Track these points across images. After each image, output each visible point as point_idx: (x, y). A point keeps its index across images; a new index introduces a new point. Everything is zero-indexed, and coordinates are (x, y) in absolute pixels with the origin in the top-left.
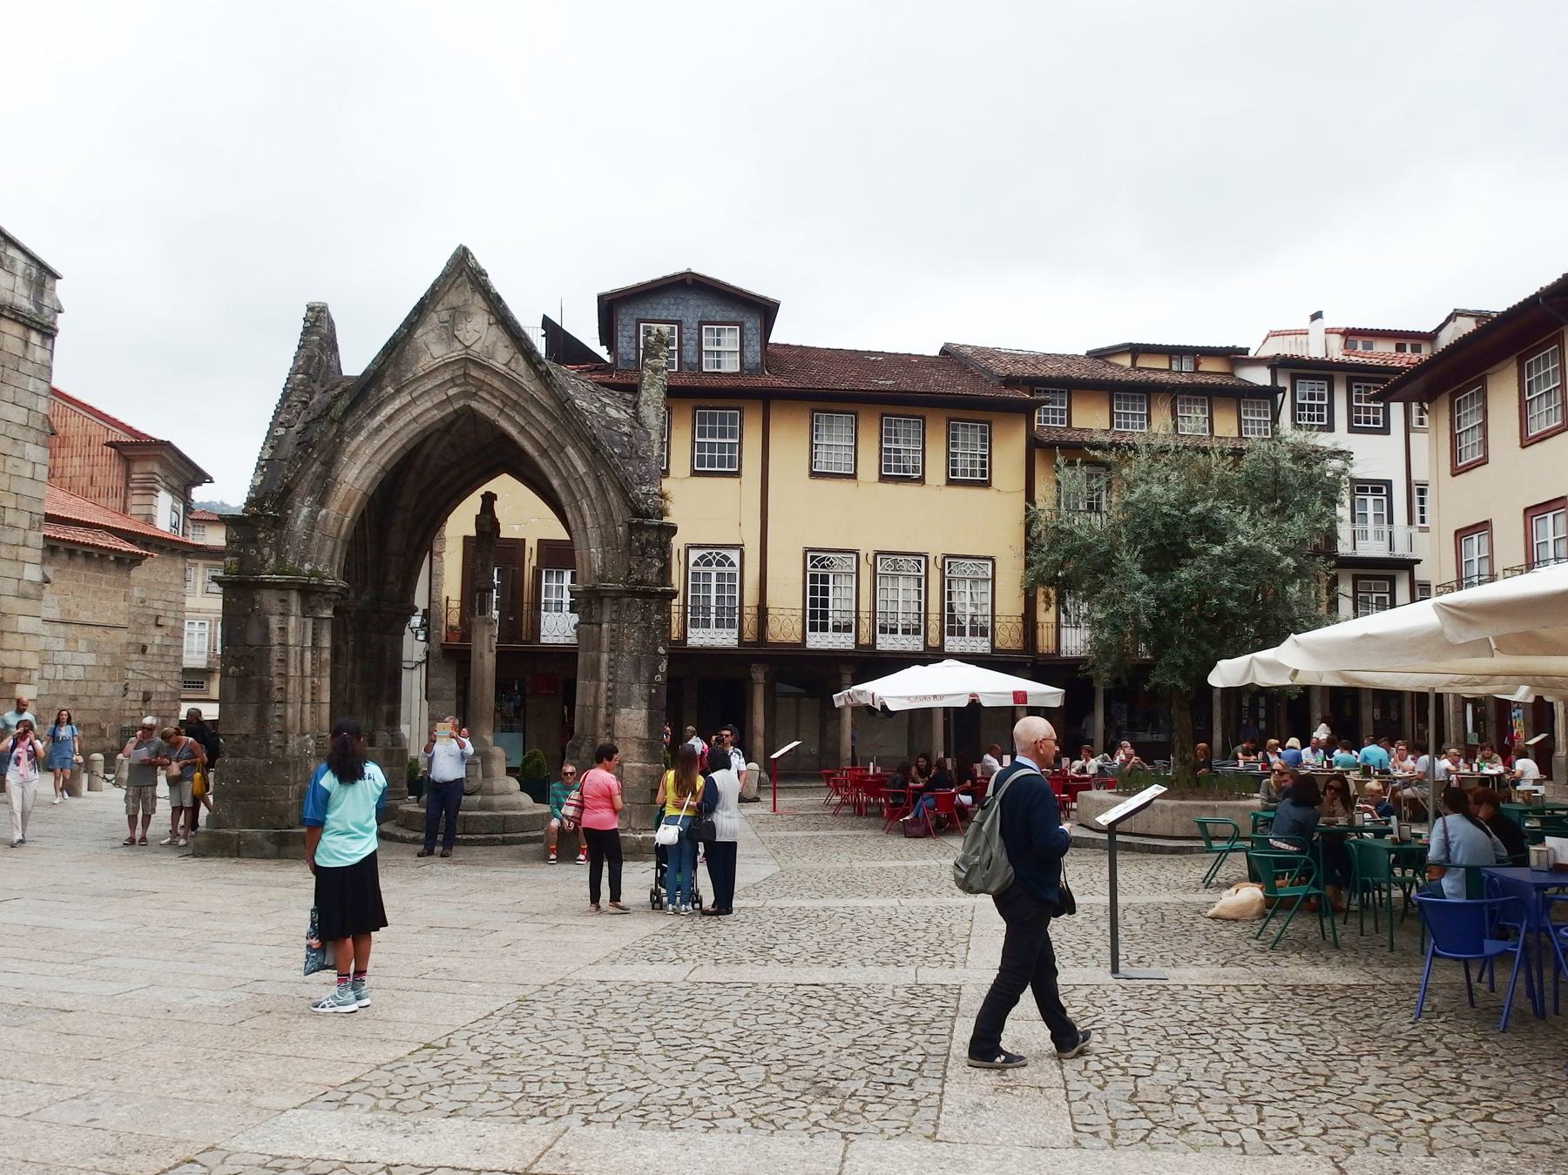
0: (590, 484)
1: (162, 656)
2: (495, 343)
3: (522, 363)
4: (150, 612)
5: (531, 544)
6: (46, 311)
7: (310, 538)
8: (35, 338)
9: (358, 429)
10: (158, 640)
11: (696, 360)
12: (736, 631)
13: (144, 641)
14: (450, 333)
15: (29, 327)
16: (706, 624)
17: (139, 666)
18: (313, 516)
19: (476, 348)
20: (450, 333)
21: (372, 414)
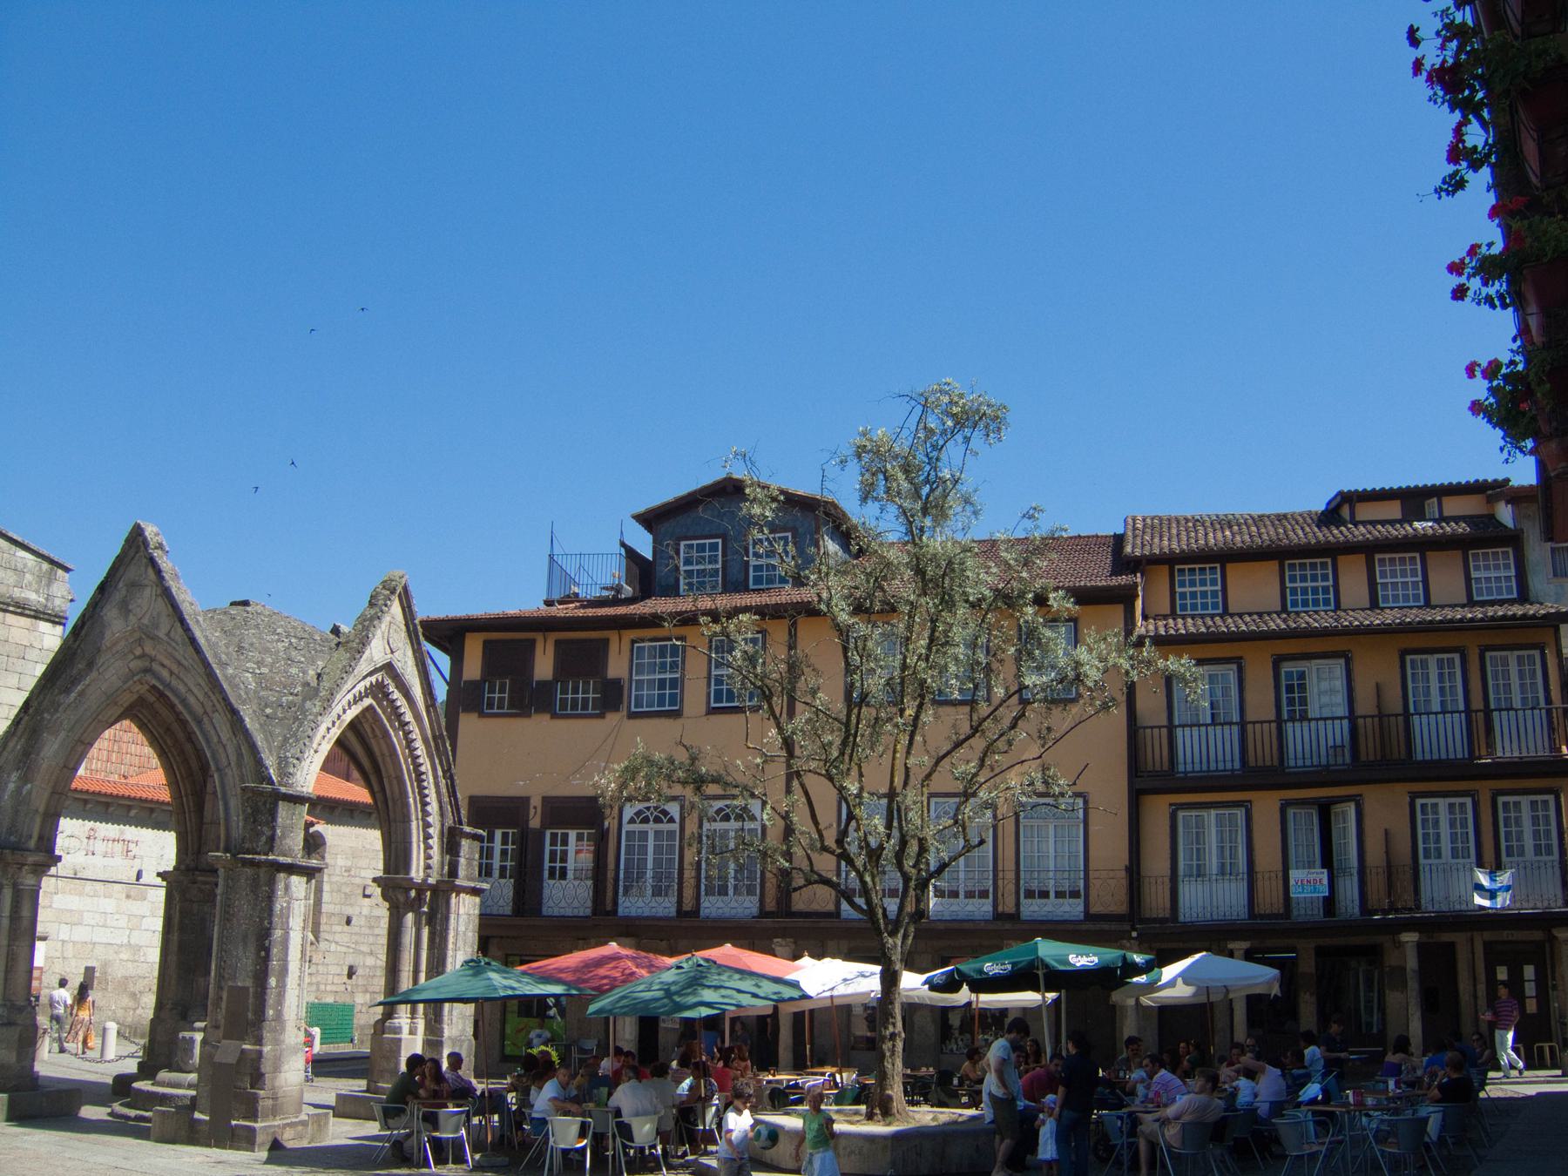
0: (231, 750)
1: (371, 927)
2: (159, 614)
3: (180, 630)
4: (357, 881)
5: (536, 802)
6: (58, 602)
7: (17, 812)
8: (44, 626)
9: (56, 706)
10: (365, 911)
11: (742, 577)
12: (756, 899)
13: (349, 911)
14: (125, 609)
15: (35, 617)
16: (723, 891)
17: (345, 938)
18: (18, 790)
19: (145, 621)
20: (125, 609)
21: (67, 691)
